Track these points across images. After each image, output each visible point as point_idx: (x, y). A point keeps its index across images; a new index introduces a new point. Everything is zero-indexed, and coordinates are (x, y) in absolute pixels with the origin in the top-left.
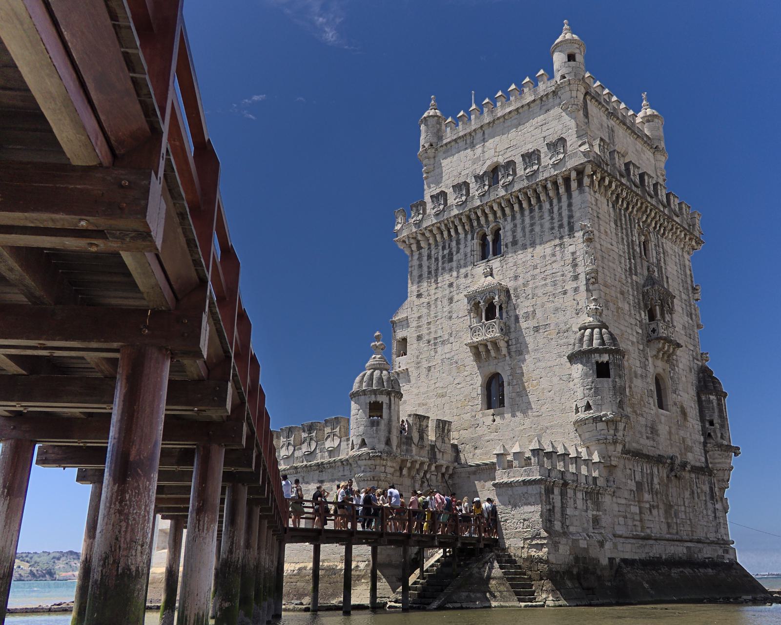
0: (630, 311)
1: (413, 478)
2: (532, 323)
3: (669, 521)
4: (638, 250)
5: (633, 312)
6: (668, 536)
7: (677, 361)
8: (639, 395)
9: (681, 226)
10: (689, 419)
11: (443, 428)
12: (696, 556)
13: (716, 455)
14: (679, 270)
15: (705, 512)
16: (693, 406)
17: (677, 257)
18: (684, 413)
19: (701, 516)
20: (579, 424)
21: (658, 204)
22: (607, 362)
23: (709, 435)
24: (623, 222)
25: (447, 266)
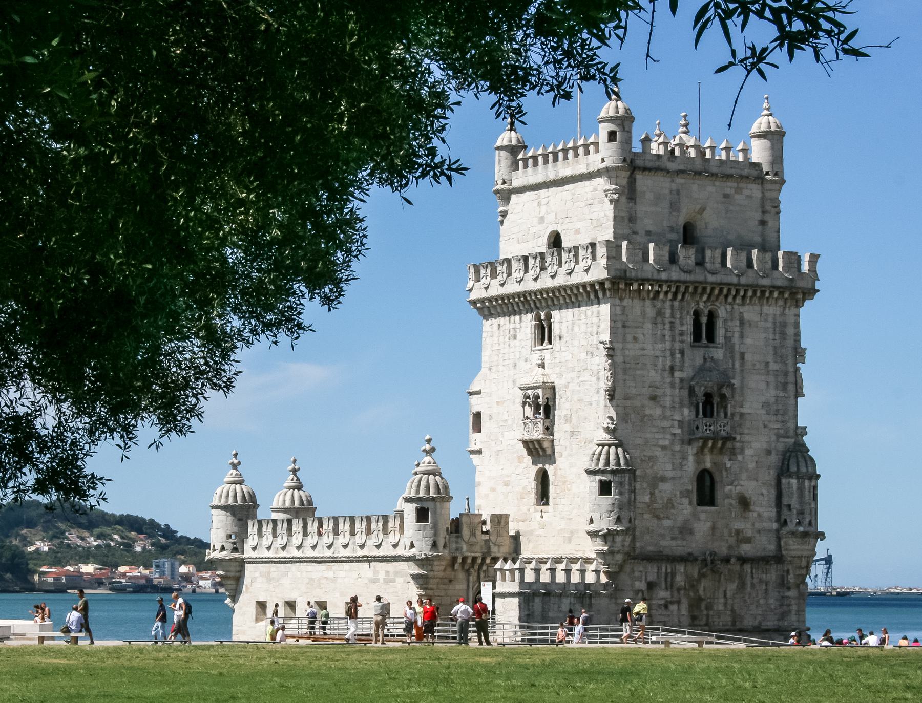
1: (468, 572)
2: (567, 427)
4: (689, 338)
5: (668, 413)
7: (742, 449)
10: (752, 508)
11: (499, 522)
13: (791, 542)
15: (762, 601)
17: (770, 319)
18: (744, 503)
19: (753, 607)
20: (589, 533)
22: (610, 482)
23: (785, 522)
24: (668, 315)
25: (512, 342)
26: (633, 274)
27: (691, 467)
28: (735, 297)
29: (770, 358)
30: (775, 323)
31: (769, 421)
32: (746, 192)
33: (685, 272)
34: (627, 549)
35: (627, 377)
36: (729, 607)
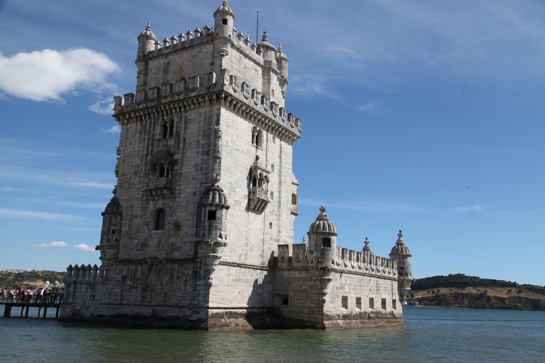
0: (140, 180)
3: (145, 295)
5: (142, 180)
6: (138, 303)
7: (179, 194)
8: (136, 228)
9: (194, 97)
10: (182, 229)
12: (160, 314)
14: (202, 125)
15: (183, 288)
16: (191, 218)
17: (203, 115)
18: (178, 226)
21: (172, 97)
24: (148, 127)
26: (126, 111)
27: (151, 207)
28: (180, 108)
29: (200, 138)
30: (205, 117)
31: (197, 175)
32: (204, 51)
33: (151, 102)
34: (107, 257)
35: (125, 164)
36: (163, 291)
